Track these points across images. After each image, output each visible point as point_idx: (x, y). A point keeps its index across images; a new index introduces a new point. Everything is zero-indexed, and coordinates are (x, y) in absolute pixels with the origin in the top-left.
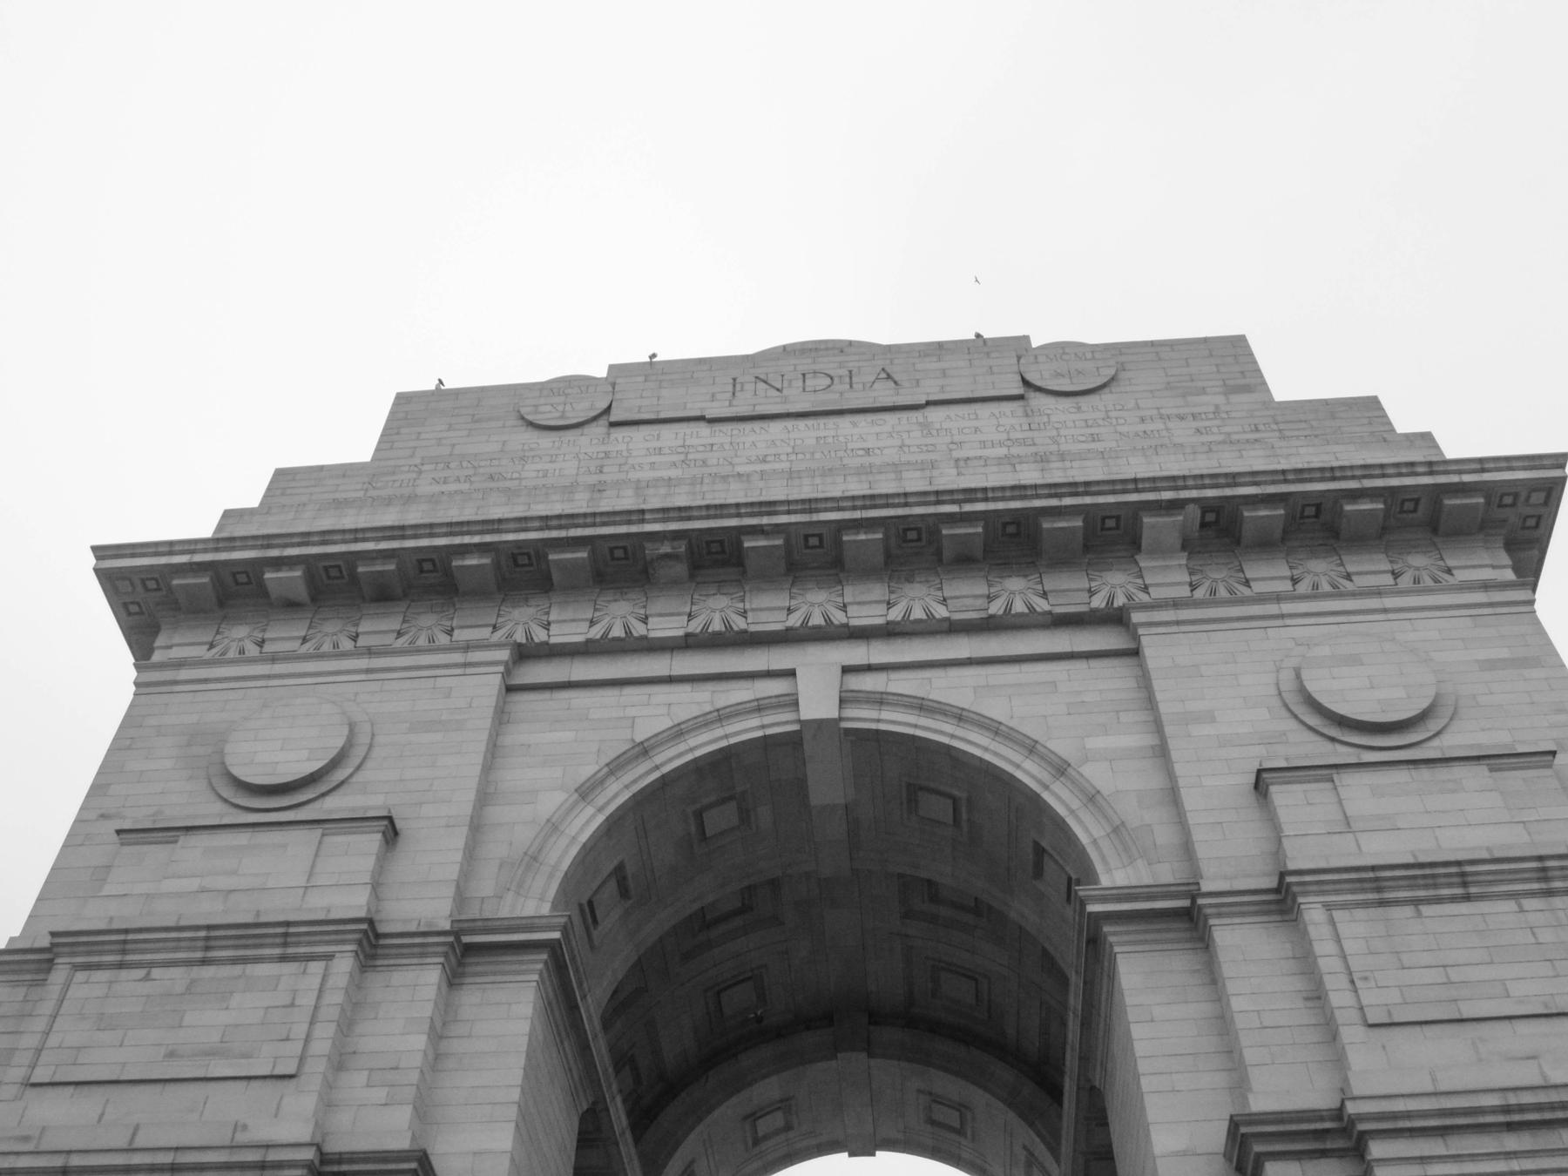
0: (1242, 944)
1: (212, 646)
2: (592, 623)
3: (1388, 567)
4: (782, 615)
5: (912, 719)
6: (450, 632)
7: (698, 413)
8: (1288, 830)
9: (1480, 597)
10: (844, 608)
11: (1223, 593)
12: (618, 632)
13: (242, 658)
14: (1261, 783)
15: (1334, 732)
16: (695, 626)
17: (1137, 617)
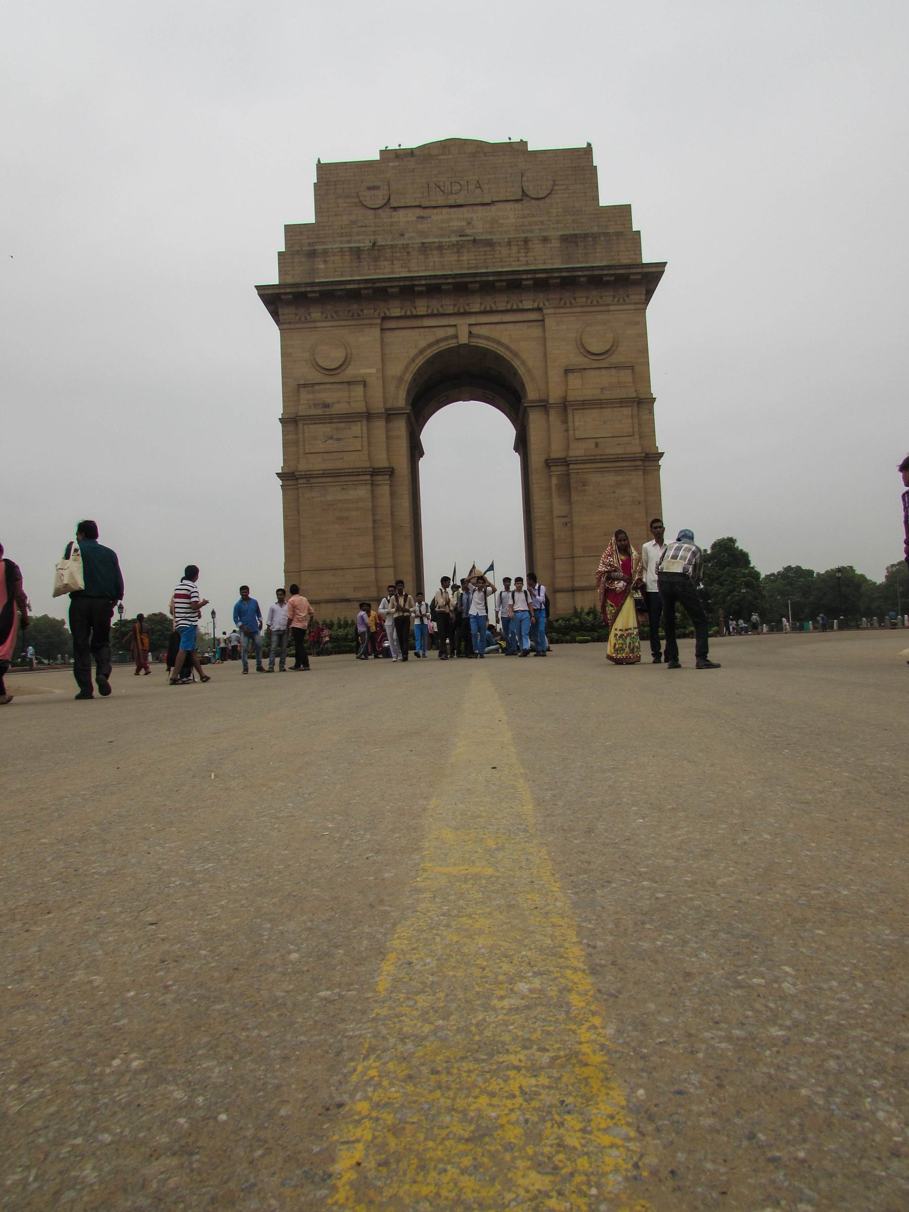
0: (554, 415)
1: (296, 315)
2: (402, 309)
3: (612, 294)
4: (452, 307)
5: (485, 342)
6: (362, 311)
7: (418, 204)
8: (570, 387)
9: (632, 307)
10: (468, 305)
11: (568, 304)
12: (409, 313)
13: (306, 321)
14: (567, 371)
15: (586, 354)
16: (430, 312)
17: (545, 311)
